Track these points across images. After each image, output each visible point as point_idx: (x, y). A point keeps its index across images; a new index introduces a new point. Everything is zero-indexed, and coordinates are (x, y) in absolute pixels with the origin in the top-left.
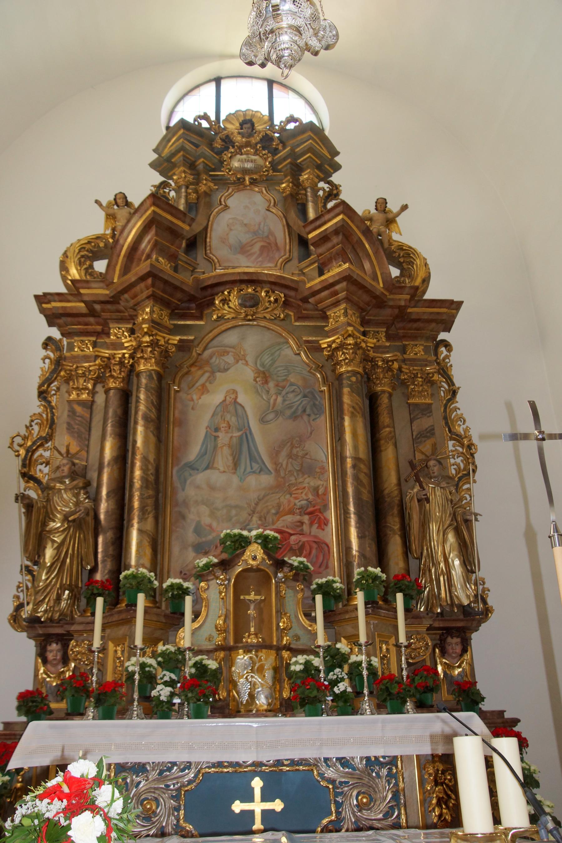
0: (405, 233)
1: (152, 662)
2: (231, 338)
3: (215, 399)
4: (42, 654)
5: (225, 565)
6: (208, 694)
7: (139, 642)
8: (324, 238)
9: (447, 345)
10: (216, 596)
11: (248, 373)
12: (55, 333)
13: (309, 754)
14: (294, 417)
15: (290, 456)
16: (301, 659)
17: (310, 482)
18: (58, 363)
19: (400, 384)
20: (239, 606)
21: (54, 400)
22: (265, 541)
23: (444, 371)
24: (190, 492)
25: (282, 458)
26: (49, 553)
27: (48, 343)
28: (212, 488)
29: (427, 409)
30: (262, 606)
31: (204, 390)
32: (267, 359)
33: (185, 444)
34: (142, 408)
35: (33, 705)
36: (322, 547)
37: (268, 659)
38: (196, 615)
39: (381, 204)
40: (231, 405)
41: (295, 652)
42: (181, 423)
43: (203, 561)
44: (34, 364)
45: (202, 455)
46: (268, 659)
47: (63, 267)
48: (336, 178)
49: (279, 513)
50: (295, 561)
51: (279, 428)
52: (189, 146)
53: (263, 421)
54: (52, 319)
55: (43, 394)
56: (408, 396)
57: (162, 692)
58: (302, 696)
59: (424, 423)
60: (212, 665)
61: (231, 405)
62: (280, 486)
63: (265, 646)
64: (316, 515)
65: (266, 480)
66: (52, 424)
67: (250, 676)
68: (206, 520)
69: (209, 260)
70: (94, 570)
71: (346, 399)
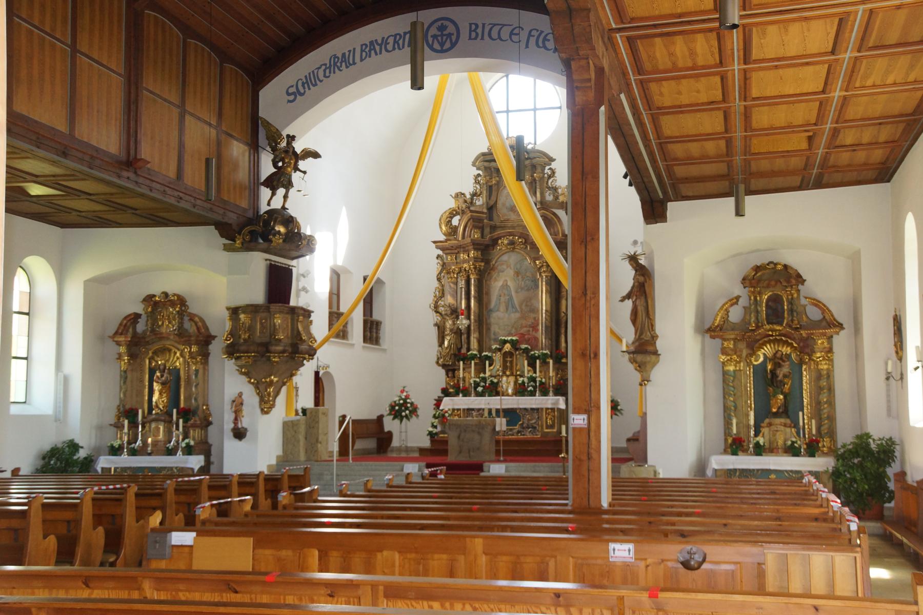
1: (478, 380)
2: (505, 258)
3: (499, 284)
4: (447, 374)
5: (500, 350)
6: (493, 390)
7: (473, 375)
10: (497, 357)
11: (511, 272)
12: (440, 252)
13: (515, 406)
14: (528, 290)
15: (526, 306)
16: (521, 379)
17: (532, 315)
18: (444, 265)
20: (505, 362)
21: (443, 281)
22: (512, 342)
24: (492, 320)
25: (523, 307)
26: (446, 343)
27: (438, 257)
28: (499, 318)
30: (511, 362)
31: (496, 280)
32: (518, 266)
33: (489, 302)
34: (473, 293)
35: (446, 392)
36: (536, 339)
37: (512, 379)
38: (490, 365)
40: (505, 286)
41: (521, 376)
42: (488, 294)
43: (494, 347)
44: (434, 267)
46: (512, 379)
47: (441, 227)
49: (522, 327)
50: (523, 346)
52: (486, 164)
53: (517, 292)
54: (437, 247)
55: (439, 279)
57: (480, 389)
58: (521, 391)
60: (495, 381)
61: (505, 286)
62: (523, 317)
63: (512, 374)
64: (534, 327)
65: (518, 315)
66: (443, 294)
67: (508, 384)
68: (497, 330)
69: (498, 216)
70: (461, 347)
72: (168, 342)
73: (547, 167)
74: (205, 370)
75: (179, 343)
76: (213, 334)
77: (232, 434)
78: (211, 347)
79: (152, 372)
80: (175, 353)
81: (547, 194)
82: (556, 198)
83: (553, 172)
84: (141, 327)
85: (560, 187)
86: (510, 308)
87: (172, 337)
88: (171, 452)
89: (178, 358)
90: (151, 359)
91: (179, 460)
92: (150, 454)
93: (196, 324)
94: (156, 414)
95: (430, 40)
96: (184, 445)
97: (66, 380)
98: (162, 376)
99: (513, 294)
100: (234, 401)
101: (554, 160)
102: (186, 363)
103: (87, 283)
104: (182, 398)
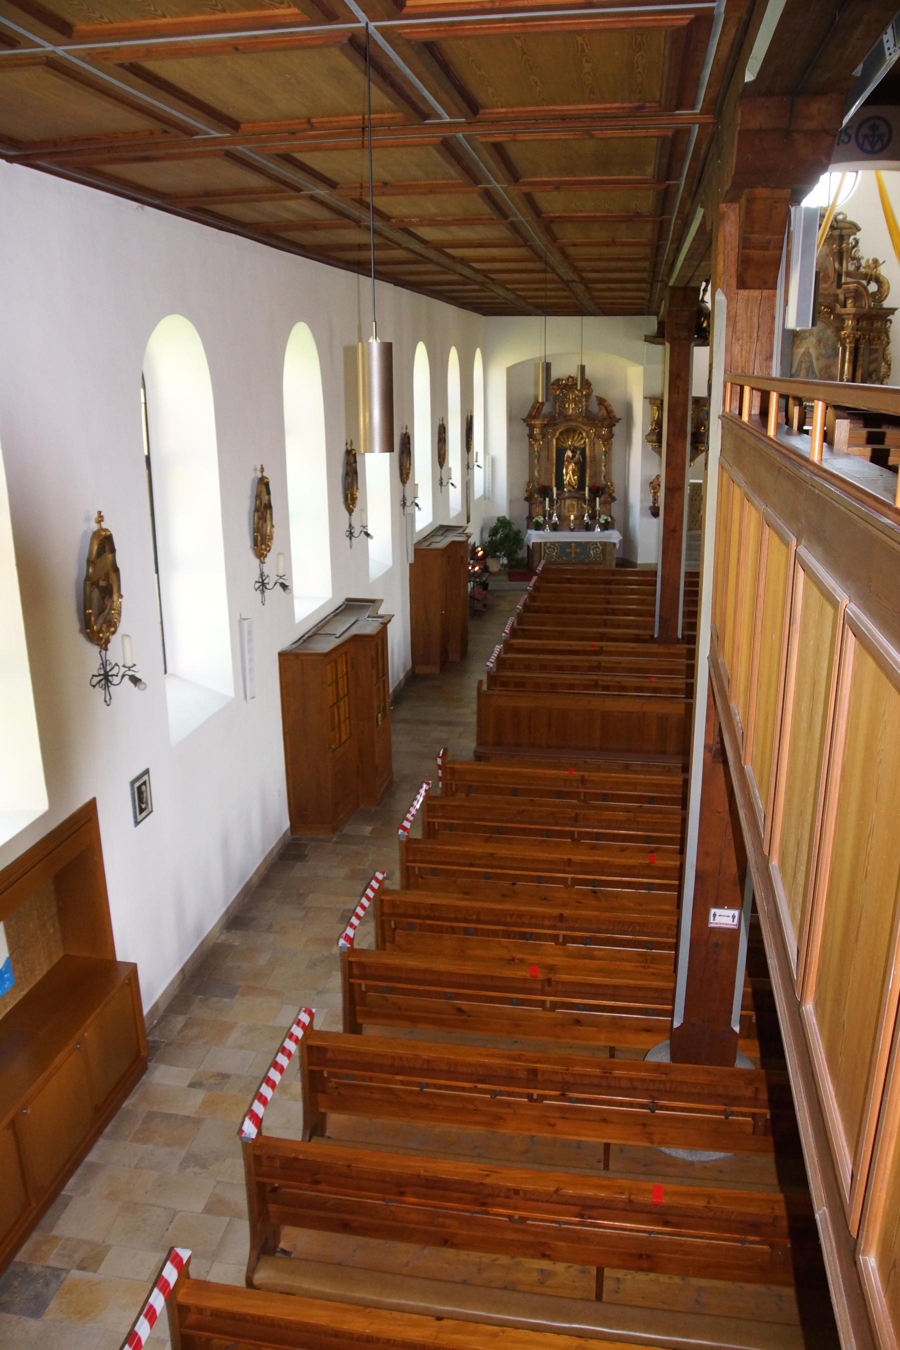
0: (883, 271)
3: (801, 350)
8: (848, 289)
9: (891, 321)
14: (829, 358)
19: (870, 342)
23: (887, 333)
29: (877, 350)
31: (798, 347)
39: (876, 261)
40: (807, 353)
45: (796, 371)
48: (858, 235)
51: (823, 362)
53: (817, 359)
56: (872, 345)
59: (874, 356)
61: (807, 353)
71: (847, 357)
72: (574, 424)
73: (852, 237)
74: (610, 449)
75: (586, 425)
76: (618, 417)
77: (649, 512)
78: (614, 429)
79: (561, 452)
80: (581, 433)
81: (850, 264)
82: (858, 268)
83: (857, 242)
84: (546, 409)
85: (862, 258)
86: (810, 374)
87: (580, 419)
88: (589, 528)
89: (582, 438)
90: (557, 439)
91: (597, 535)
92: (572, 530)
93: (606, 408)
94: (569, 491)
95: (861, 141)
96: (602, 521)
97: (493, 461)
98: (574, 456)
99: (814, 361)
100: (651, 483)
101: (859, 229)
102: (593, 444)
103: (510, 370)
104: (587, 475)
